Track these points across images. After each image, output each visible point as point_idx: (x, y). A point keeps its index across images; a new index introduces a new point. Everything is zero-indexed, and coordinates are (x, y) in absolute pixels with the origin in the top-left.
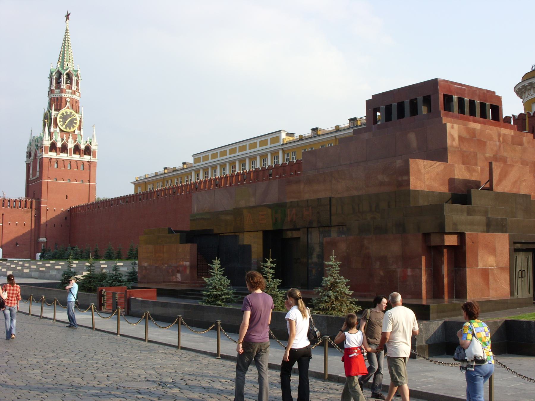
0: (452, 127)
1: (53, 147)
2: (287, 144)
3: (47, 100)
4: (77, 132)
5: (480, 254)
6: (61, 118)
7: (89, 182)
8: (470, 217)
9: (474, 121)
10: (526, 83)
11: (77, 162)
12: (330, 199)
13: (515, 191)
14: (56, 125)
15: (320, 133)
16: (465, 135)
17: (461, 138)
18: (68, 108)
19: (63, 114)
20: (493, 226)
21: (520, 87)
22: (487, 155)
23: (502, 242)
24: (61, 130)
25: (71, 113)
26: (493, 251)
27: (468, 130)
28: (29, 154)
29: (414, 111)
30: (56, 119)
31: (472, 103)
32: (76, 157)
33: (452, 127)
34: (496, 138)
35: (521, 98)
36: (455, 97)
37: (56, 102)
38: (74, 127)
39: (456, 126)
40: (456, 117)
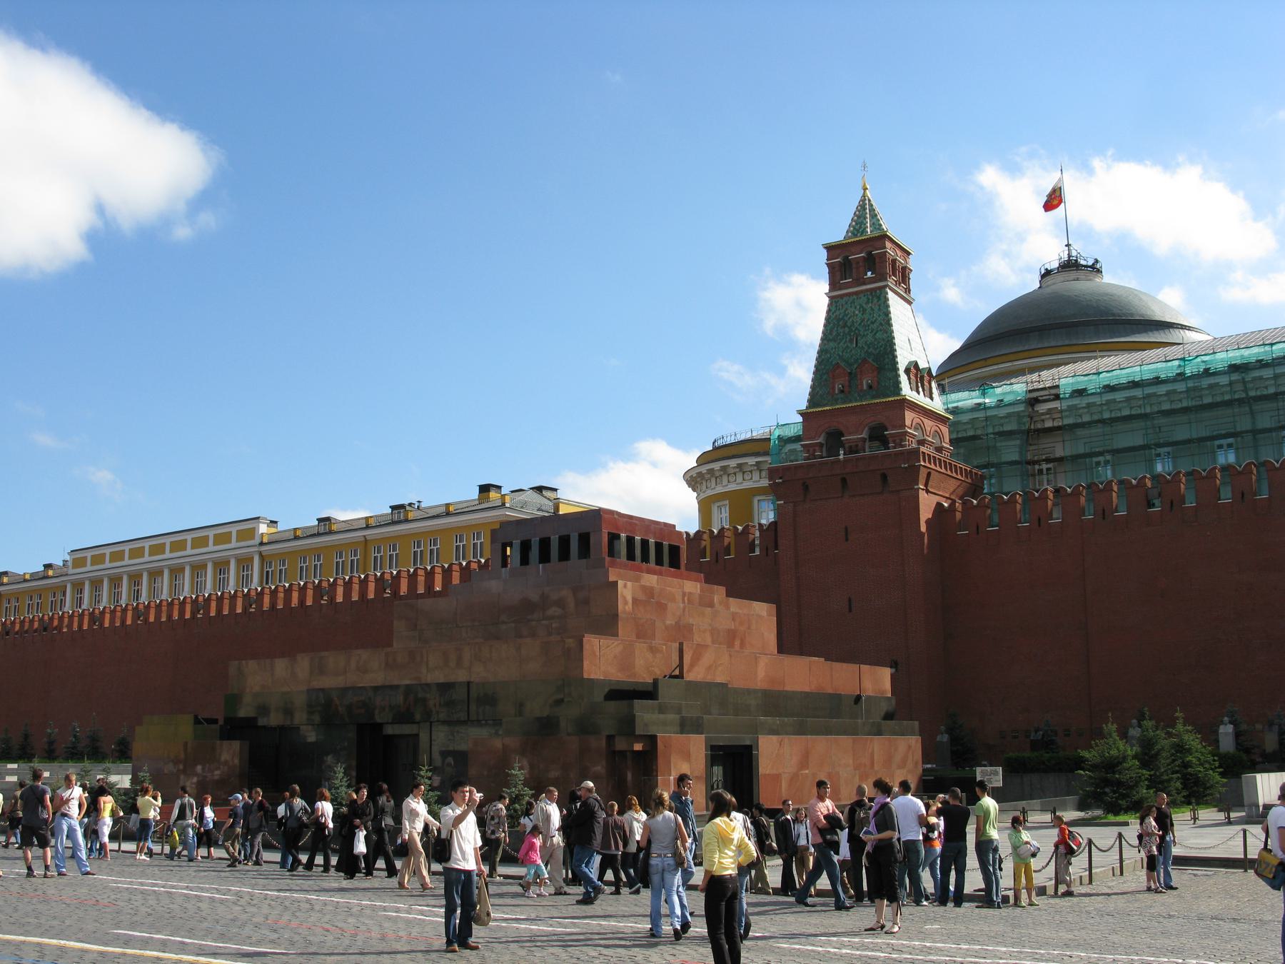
0: (625, 586)
2: (269, 543)
5: (673, 760)
8: (662, 716)
9: (649, 572)
10: (704, 469)
12: (469, 683)
13: (709, 679)
15: (334, 527)
16: (641, 597)
17: (635, 601)
20: (688, 726)
21: (694, 473)
22: (668, 622)
23: (697, 746)
26: (687, 756)
27: (644, 588)
29: (564, 555)
31: (645, 543)
33: (625, 586)
34: (679, 598)
35: (694, 490)
36: (623, 535)
39: (629, 584)
40: (625, 567)
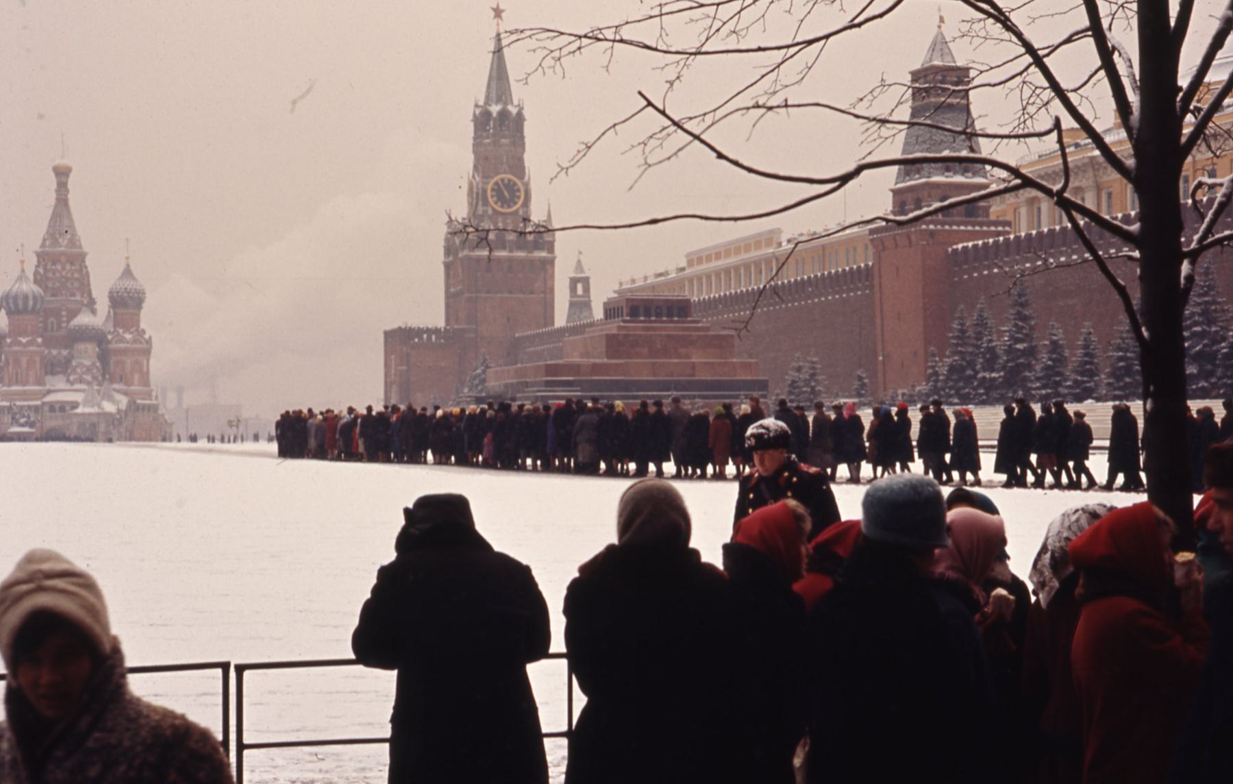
1: (483, 240)
3: (469, 159)
4: (521, 212)
6: (493, 190)
7: (545, 293)
11: (521, 261)
14: (486, 203)
18: (505, 172)
19: (496, 183)
24: (494, 210)
25: (510, 180)
28: (448, 250)
30: (484, 191)
32: (521, 254)
37: (484, 163)
38: (515, 203)
